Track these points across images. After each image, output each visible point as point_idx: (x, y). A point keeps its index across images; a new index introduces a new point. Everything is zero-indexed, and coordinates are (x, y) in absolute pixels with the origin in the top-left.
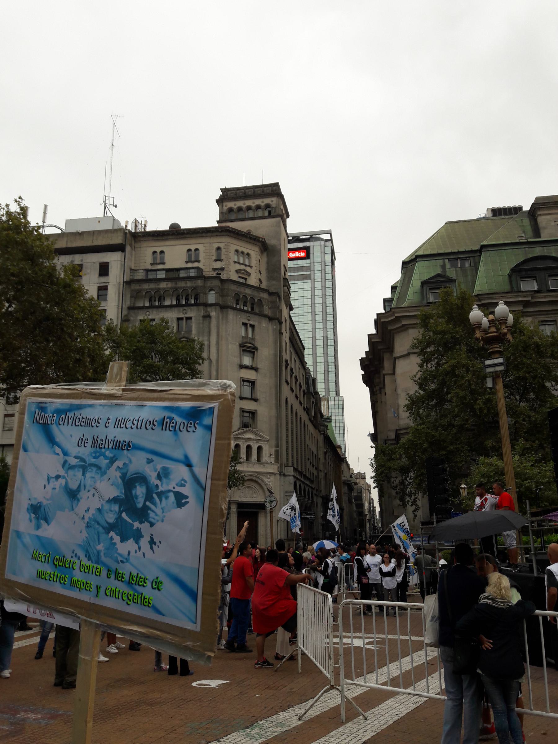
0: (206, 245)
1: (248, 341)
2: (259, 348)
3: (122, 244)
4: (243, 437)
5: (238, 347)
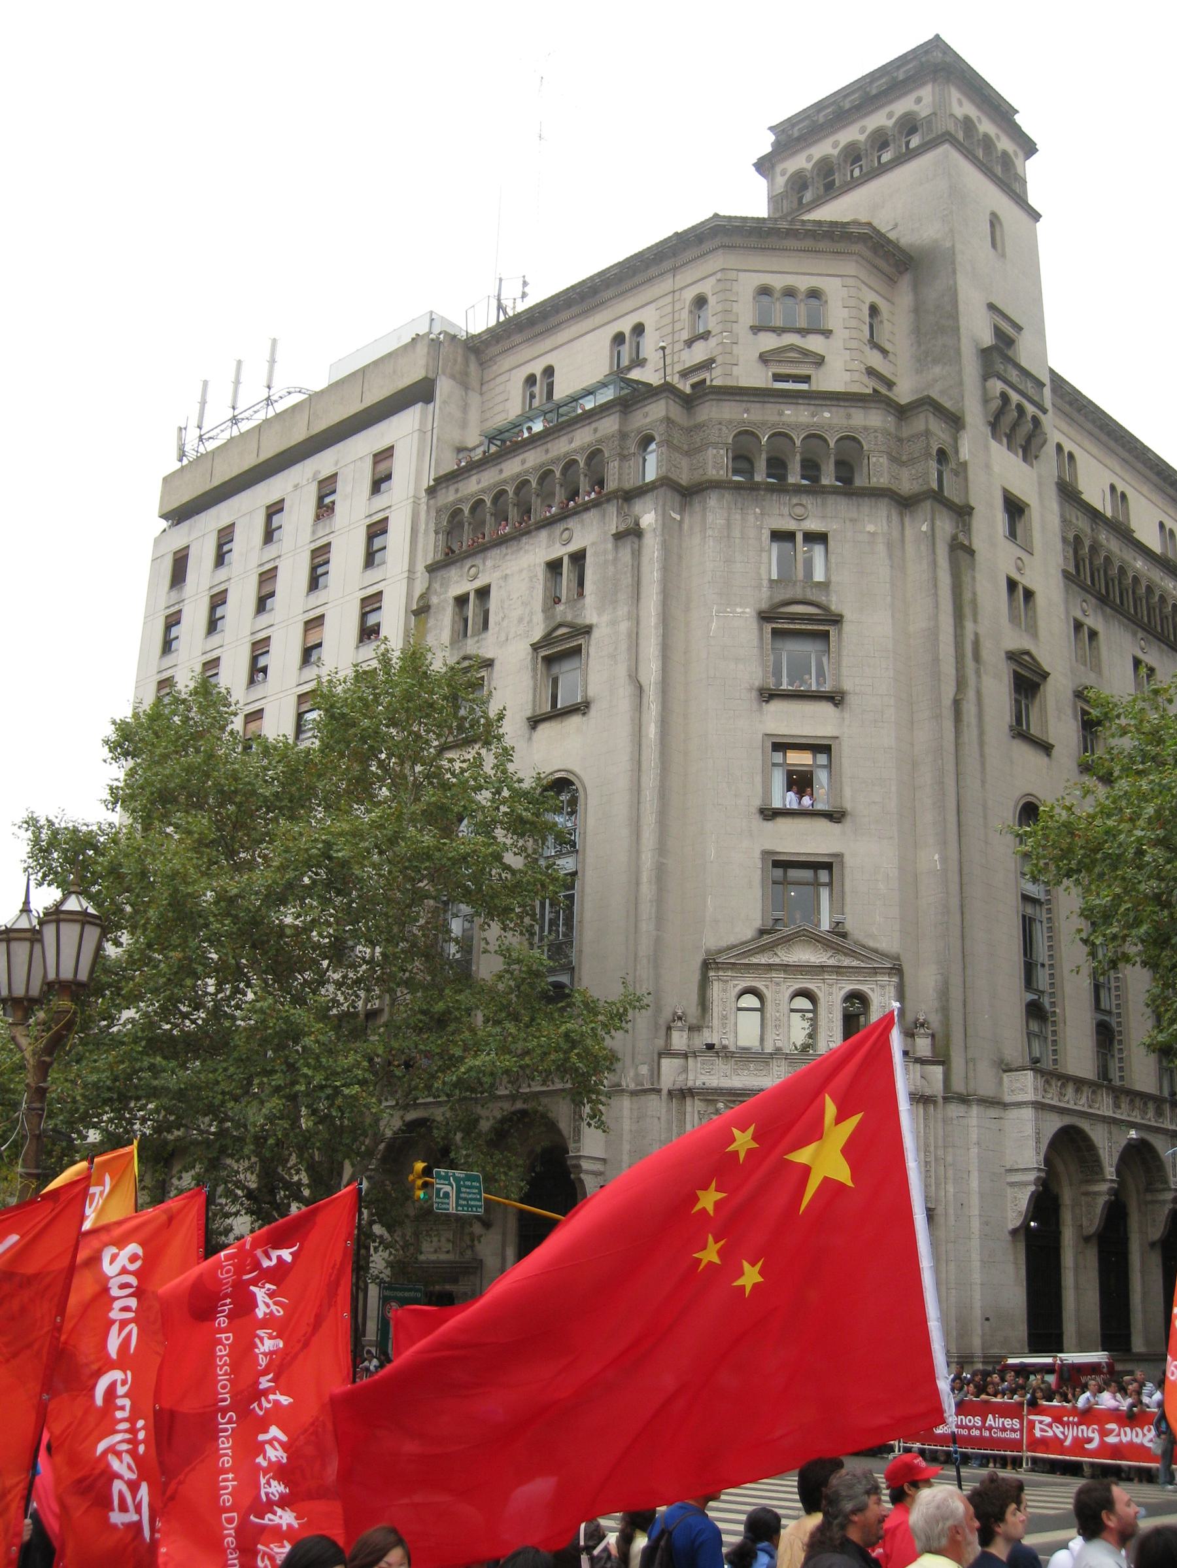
0: (661, 302)
1: (799, 595)
2: (848, 615)
3: (425, 379)
4: (777, 961)
5: (753, 624)
